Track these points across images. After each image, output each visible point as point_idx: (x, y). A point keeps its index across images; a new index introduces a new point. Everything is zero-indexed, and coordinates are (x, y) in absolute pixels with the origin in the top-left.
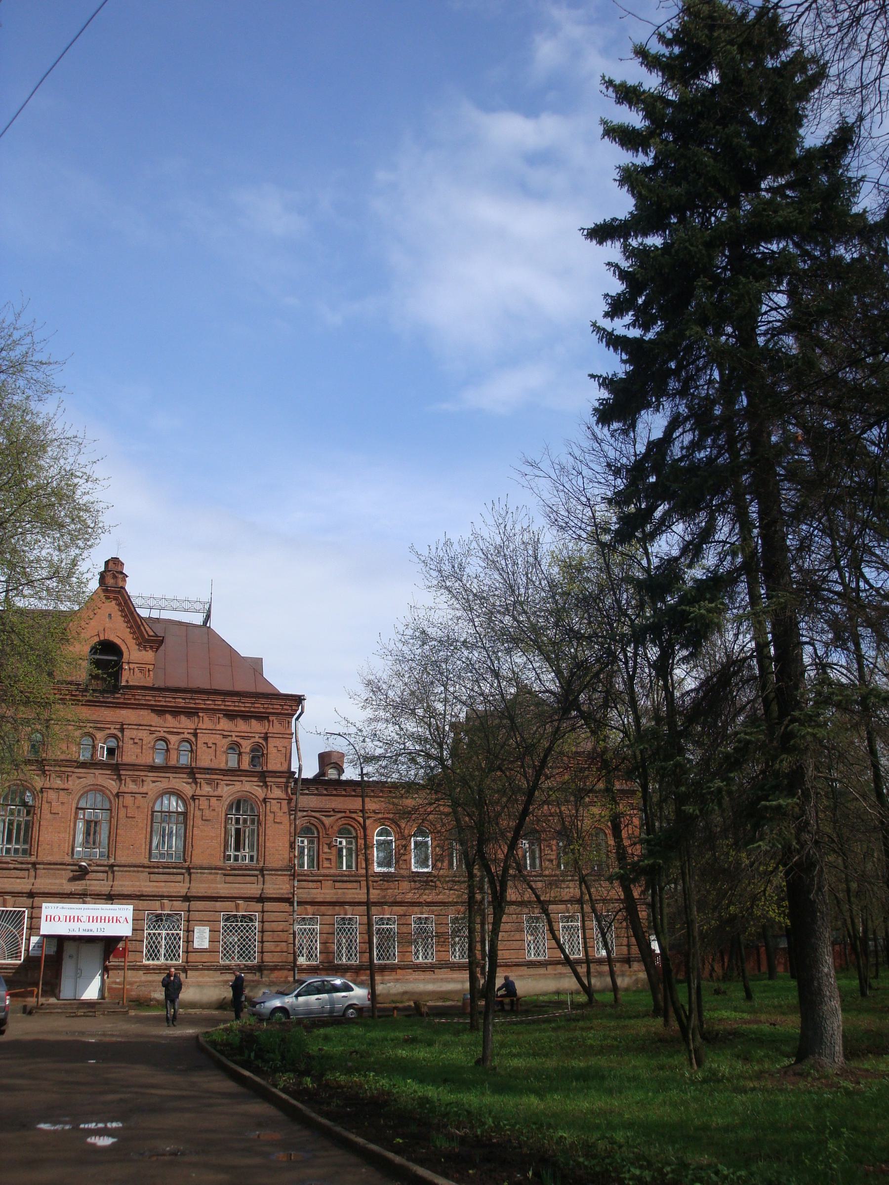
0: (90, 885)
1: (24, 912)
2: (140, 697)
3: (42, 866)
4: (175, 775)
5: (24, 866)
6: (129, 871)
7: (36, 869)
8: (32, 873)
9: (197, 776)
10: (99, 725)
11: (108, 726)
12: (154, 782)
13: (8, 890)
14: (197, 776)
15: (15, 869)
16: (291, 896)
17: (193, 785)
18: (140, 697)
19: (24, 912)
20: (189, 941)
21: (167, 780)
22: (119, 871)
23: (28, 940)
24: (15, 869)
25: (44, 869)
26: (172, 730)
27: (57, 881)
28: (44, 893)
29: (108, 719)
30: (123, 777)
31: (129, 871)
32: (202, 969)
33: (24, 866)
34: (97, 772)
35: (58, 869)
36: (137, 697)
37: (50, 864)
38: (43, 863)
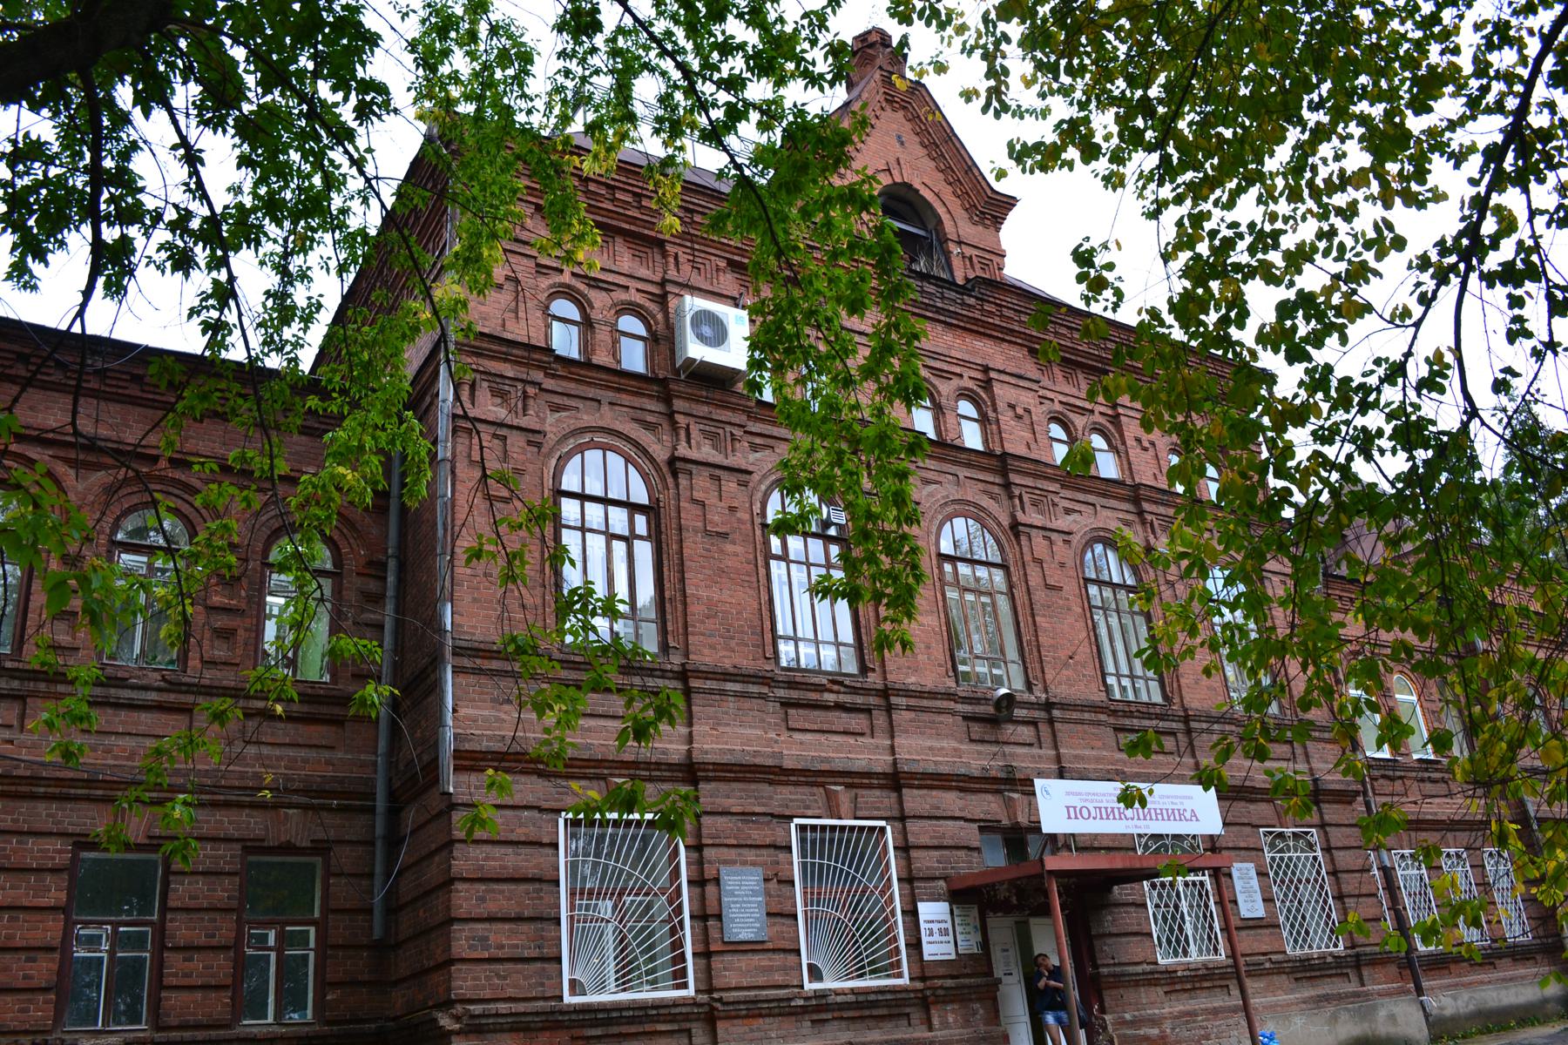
0: (1012, 755)
1: (883, 830)
2: (1010, 314)
3: (902, 701)
4: (1104, 501)
5: (859, 700)
6: (1081, 722)
7: (889, 709)
8: (880, 720)
9: (1146, 506)
10: (938, 364)
11: (958, 370)
12: (1068, 511)
13: (839, 766)
14: (1146, 506)
15: (839, 707)
16: (1360, 787)
17: (1139, 528)
18: (1010, 314)
19: (883, 830)
20: (1227, 902)
21: (1090, 509)
22: (1068, 721)
23: (912, 913)
24: (839, 707)
25: (909, 708)
26: (1072, 401)
28: (926, 775)
30: (1017, 492)
32: (1269, 973)
33: (859, 700)
34: (963, 472)
35: (940, 711)
36: (1006, 312)
37: (920, 694)
38: (908, 693)
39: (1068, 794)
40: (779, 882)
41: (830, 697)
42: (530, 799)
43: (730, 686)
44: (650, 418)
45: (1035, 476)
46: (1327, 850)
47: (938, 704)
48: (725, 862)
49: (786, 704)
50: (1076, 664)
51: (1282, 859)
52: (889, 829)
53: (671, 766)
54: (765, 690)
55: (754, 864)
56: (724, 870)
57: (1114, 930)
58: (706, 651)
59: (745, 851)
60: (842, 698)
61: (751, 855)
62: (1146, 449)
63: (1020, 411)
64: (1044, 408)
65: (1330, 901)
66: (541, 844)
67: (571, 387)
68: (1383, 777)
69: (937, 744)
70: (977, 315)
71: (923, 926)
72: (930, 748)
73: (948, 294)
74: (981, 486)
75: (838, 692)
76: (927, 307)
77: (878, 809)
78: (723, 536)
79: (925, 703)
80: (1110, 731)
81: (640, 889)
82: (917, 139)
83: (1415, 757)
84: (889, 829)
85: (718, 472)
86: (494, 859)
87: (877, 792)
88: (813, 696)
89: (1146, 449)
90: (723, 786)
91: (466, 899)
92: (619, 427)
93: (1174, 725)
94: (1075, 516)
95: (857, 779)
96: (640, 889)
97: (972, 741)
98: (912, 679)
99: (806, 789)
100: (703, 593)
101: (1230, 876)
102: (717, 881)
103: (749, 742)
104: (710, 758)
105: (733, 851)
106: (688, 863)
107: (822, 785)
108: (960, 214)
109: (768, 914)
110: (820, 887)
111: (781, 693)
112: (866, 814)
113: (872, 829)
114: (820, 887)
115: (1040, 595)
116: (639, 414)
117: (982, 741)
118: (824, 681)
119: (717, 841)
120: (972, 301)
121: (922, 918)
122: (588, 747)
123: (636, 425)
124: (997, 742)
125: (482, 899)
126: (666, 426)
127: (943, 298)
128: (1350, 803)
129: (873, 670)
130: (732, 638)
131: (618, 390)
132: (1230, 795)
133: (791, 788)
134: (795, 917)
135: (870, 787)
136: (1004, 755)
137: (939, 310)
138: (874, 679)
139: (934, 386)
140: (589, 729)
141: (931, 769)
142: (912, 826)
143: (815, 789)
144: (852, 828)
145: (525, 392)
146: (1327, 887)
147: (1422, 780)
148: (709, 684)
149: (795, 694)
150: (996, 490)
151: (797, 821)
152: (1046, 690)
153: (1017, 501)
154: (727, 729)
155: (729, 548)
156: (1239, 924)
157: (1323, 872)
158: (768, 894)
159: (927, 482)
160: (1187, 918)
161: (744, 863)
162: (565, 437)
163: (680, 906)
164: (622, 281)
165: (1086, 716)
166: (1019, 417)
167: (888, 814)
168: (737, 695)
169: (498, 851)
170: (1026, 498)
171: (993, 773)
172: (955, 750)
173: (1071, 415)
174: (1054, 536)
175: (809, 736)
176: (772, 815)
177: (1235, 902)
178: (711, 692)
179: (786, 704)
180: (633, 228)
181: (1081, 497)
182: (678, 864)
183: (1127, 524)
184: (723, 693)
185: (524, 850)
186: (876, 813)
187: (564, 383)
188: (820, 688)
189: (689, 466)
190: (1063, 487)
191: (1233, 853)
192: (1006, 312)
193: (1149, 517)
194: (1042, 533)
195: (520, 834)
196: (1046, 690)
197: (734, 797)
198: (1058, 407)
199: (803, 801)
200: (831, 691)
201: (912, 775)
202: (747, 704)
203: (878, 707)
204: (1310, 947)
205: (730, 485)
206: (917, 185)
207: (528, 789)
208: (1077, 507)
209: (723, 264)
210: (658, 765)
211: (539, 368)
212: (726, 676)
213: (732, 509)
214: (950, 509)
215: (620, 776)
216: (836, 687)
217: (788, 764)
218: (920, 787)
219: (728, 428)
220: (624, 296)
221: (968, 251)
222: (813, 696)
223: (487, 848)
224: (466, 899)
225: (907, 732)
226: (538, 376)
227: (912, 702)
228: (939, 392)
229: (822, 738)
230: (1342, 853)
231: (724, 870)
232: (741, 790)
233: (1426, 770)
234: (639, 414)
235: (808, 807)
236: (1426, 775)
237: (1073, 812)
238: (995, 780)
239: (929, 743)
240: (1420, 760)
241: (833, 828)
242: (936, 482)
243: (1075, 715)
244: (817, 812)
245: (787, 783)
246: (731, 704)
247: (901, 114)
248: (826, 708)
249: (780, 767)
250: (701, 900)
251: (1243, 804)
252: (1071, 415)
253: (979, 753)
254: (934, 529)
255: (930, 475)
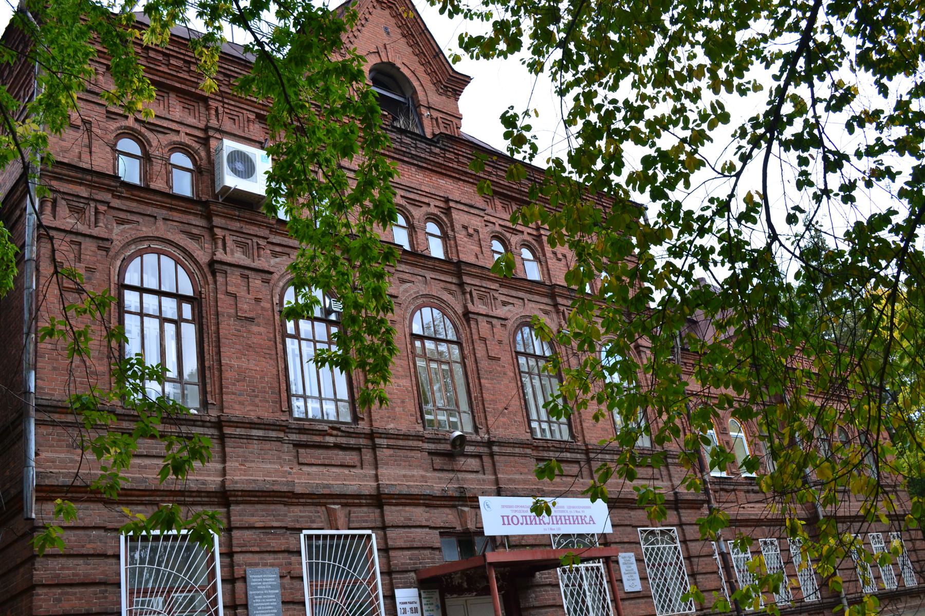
0: (463, 480)
1: (369, 536)
3: (384, 442)
5: (352, 441)
6: (513, 455)
7: (374, 447)
8: (368, 455)
9: (560, 300)
11: (426, 200)
12: (505, 304)
13: (337, 490)
14: (560, 300)
17: (554, 316)
18: (465, 160)
19: (369, 536)
20: (615, 581)
23: (390, 598)
25: (389, 447)
27: (415, 472)
29: (423, 188)
30: (468, 289)
31: (513, 455)
33: (352, 441)
34: (429, 275)
35: (412, 449)
36: (462, 159)
37: (397, 437)
38: (388, 435)
39: (503, 507)
40: (292, 578)
41: (330, 440)
42: (98, 521)
43: (255, 432)
44: (195, 231)
45: (481, 278)
46: (684, 542)
47: (410, 443)
48: (251, 565)
49: (298, 445)
50: (510, 413)
51: (653, 549)
52: (374, 536)
53: (209, 494)
54: (281, 435)
55: (272, 565)
56: (249, 571)
57: (537, 604)
58: (236, 406)
59: (266, 556)
60: (340, 440)
61: (269, 558)
62: (559, 260)
63: (471, 231)
64: (488, 229)
65: (686, 578)
66: (105, 556)
67: (133, 206)
68: (722, 490)
69: (409, 473)
70: (441, 161)
71: (399, 606)
72: (404, 476)
73: (419, 144)
74: (442, 285)
75: (336, 436)
76: (404, 153)
77: (366, 521)
78: (251, 320)
79: (401, 443)
80: (534, 461)
81: (185, 587)
82: (399, 31)
83: (743, 476)
84: (374, 536)
85: (246, 272)
86: (68, 569)
87: (365, 509)
88: (318, 439)
89: (559, 260)
90: (248, 508)
91: (45, 600)
92: (170, 236)
93: (579, 456)
94: (510, 307)
95: (350, 500)
96: (185, 587)
97: (435, 470)
98: (392, 426)
99: (312, 508)
100: (235, 363)
101: (617, 562)
102: (244, 579)
103: (269, 473)
104: (239, 487)
105: (257, 556)
106: (222, 567)
107: (325, 505)
108: (430, 87)
109: (283, 602)
110: (322, 581)
111: (294, 437)
112: (357, 525)
113: (361, 536)
114: (322, 581)
115: (484, 364)
116: (187, 228)
117: (442, 470)
118: (326, 428)
119: (244, 549)
120: (437, 150)
121: (398, 600)
122: (144, 480)
123: (184, 236)
124: (453, 471)
125: (59, 600)
126: (207, 237)
127: (416, 147)
128: (699, 509)
129: (363, 419)
130: (256, 396)
131: (171, 209)
132: (614, 504)
133: (301, 508)
134: (303, 603)
135: (360, 505)
136: (458, 479)
137: (413, 157)
138: (363, 426)
139: (409, 211)
140: (145, 467)
141: (405, 491)
142: (391, 533)
143: (319, 508)
144: (346, 536)
145: (96, 208)
146: (684, 568)
147: (748, 492)
148: (239, 431)
149: (304, 438)
150: (453, 287)
151: (305, 532)
152: (488, 432)
153: (468, 296)
154: (253, 465)
155: (255, 329)
156: (624, 596)
157: (681, 557)
158: (283, 587)
159: (403, 281)
160: (588, 593)
161: (265, 565)
162: (128, 244)
163: (216, 599)
164: (174, 126)
165: (517, 450)
166: (470, 235)
167: (373, 525)
168: (260, 439)
169: (71, 562)
170: (474, 293)
171: (450, 493)
172: (422, 476)
173: (508, 235)
174: (494, 321)
175: (314, 469)
176: (286, 528)
177: (621, 581)
178: (240, 437)
179: (298, 445)
180: (183, 87)
181: (514, 293)
182: (214, 568)
183: (546, 313)
184: (249, 437)
185: (92, 561)
186: (364, 525)
187: (128, 203)
188: (323, 433)
189: (225, 267)
190: (501, 286)
191: (619, 546)
192: (462, 159)
193: (561, 308)
194: (485, 319)
195: (89, 548)
196: (488, 432)
197: (256, 515)
198: (498, 228)
199: (310, 517)
200: (331, 435)
201: (391, 496)
202: (268, 445)
203: (366, 446)
204: (673, 611)
205: (256, 282)
206: (398, 65)
207: (95, 514)
208: (511, 300)
209: (252, 117)
210: (199, 493)
211: (108, 190)
212: (252, 425)
213: (258, 300)
214: (420, 301)
215: (169, 502)
216: (335, 432)
217: (298, 490)
218: (396, 505)
219: (255, 240)
220: (175, 138)
221: (435, 114)
222: (318, 439)
223: (62, 560)
224: (45, 600)
225: (387, 464)
226: (108, 197)
227: (392, 442)
228: (412, 216)
229: (324, 470)
230: (694, 544)
231: (249, 571)
232: (264, 510)
233: (751, 484)
234: (187, 228)
235: (313, 522)
236: (751, 488)
237: (507, 520)
238: (452, 498)
239: (403, 472)
240: (746, 478)
241: (332, 536)
242: (410, 282)
243: (509, 450)
244: (320, 525)
245: (298, 504)
246: (255, 446)
247: (387, 11)
248: (326, 447)
249: (293, 492)
250: (231, 594)
251: (626, 511)
252: (508, 235)
253: (440, 478)
254: (408, 316)
255: (406, 277)
